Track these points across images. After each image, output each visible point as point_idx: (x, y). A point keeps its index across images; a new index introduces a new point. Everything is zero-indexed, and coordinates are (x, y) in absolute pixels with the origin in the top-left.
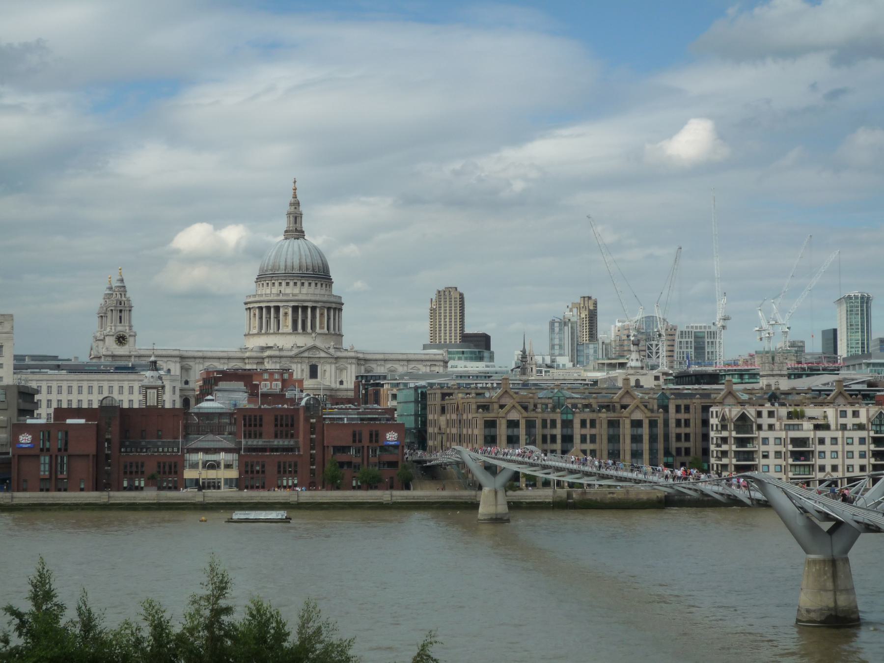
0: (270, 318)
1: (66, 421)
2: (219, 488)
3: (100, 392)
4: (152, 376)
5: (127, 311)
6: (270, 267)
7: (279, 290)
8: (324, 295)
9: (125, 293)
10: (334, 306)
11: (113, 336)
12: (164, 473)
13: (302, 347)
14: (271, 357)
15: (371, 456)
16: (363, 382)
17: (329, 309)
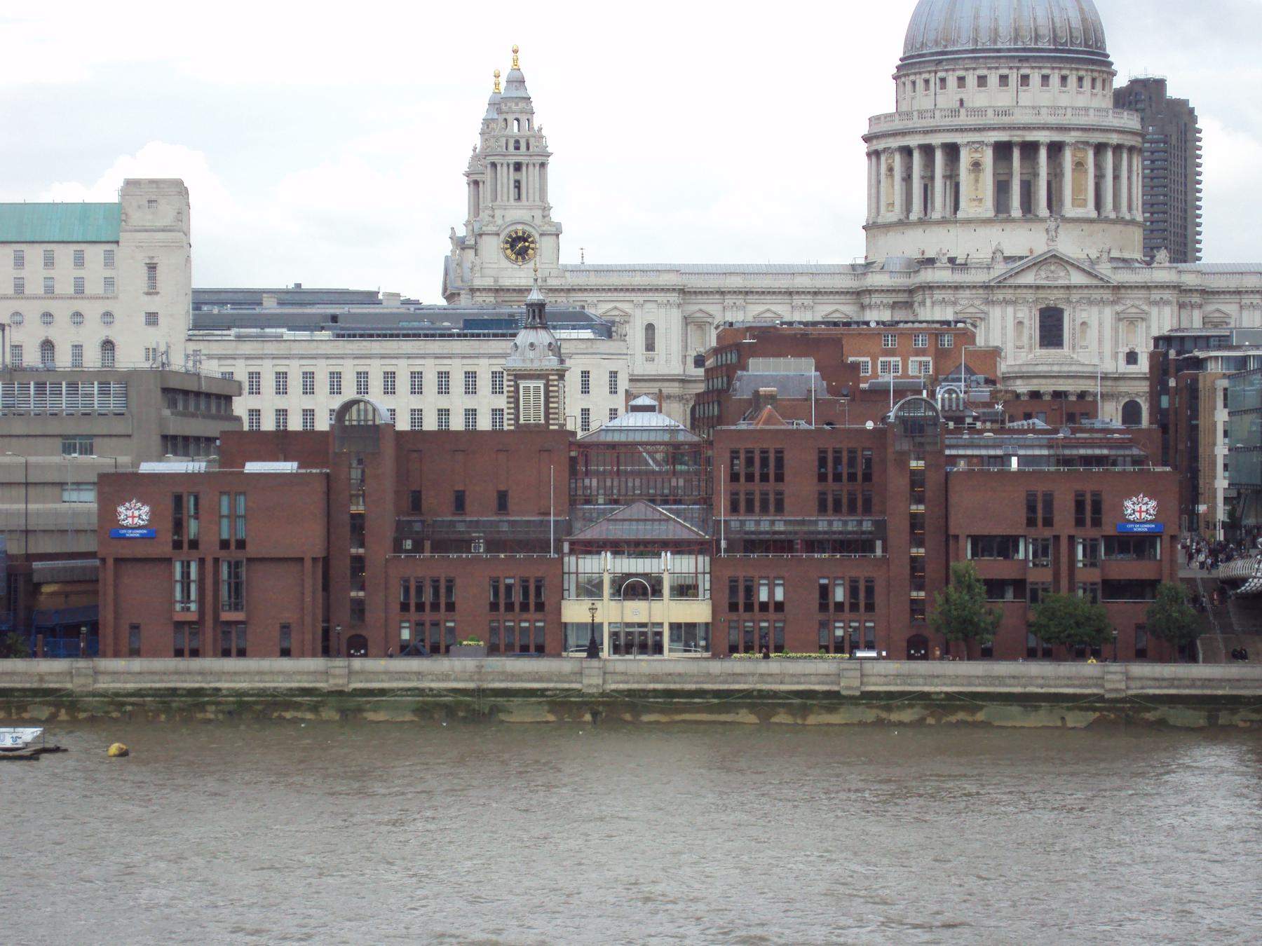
0: (932, 178)
1: (243, 466)
2: (658, 649)
3: (336, 388)
4: (532, 345)
5: (534, 165)
6: (932, 36)
7: (958, 97)
8: (1086, 109)
9: (529, 116)
10: (1114, 139)
11: (498, 235)
12: (510, 607)
13: (1021, 258)
14: (931, 288)
15: (1080, 565)
16: (1172, 354)
17: (1100, 148)
